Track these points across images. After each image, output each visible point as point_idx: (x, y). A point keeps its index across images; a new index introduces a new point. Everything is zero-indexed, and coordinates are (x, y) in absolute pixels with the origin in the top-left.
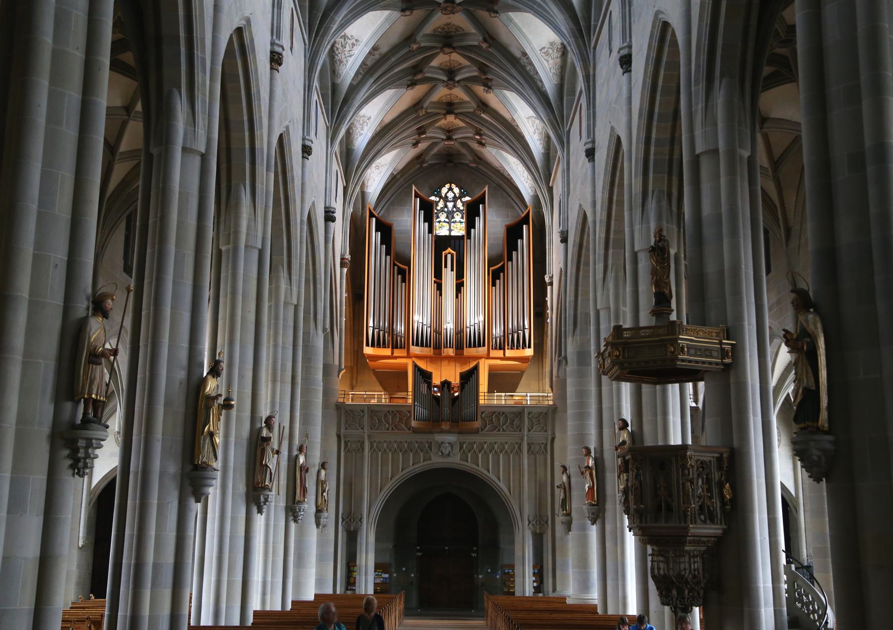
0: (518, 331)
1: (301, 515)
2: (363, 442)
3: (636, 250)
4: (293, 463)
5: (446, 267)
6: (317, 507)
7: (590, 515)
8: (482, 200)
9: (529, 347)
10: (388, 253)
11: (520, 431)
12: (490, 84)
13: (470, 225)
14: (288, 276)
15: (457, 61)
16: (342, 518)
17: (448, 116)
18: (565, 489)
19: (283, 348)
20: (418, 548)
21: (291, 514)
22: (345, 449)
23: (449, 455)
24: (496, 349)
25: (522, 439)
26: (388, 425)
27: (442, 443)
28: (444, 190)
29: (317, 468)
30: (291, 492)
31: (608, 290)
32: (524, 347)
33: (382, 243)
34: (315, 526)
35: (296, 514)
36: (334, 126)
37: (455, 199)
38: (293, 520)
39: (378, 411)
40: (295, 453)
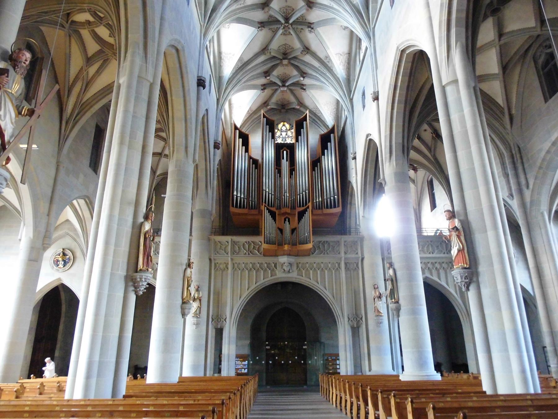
0: (330, 197)
1: (142, 285)
2: (228, 264)
3: (444, 83)
4: (136, 230)
5: (283, 158)
6: (183, 299)
7: (463, 280)
8: (305, 119)
9: (338, 206)
10: (247, 150)
11: (339, 253)
12: (312, 26)
13: (298, 133)
14: (144, 55)
15: (291, 7)
16: (212, 318)
17: (284, 61)
18: (392, 281)
19: (134, 117)
20: (267, 343)
21: (131, 283)
22: (214, 269)
23: (289, 272)
24: (316, 209)
25: (341, 261)
26: (245, 251)
27: (284, 263)
28: (280, 126)
29: (184, 267)
30: (133, 261)
31: (454, 66)
32: (335, 207)
33: (242, 146)
34: (181, 315)
35: (136, 284)
36: (206, 27)
37: (287, 131)
38: (133, 290)
39: (238, 242)
40: (141, 220)
